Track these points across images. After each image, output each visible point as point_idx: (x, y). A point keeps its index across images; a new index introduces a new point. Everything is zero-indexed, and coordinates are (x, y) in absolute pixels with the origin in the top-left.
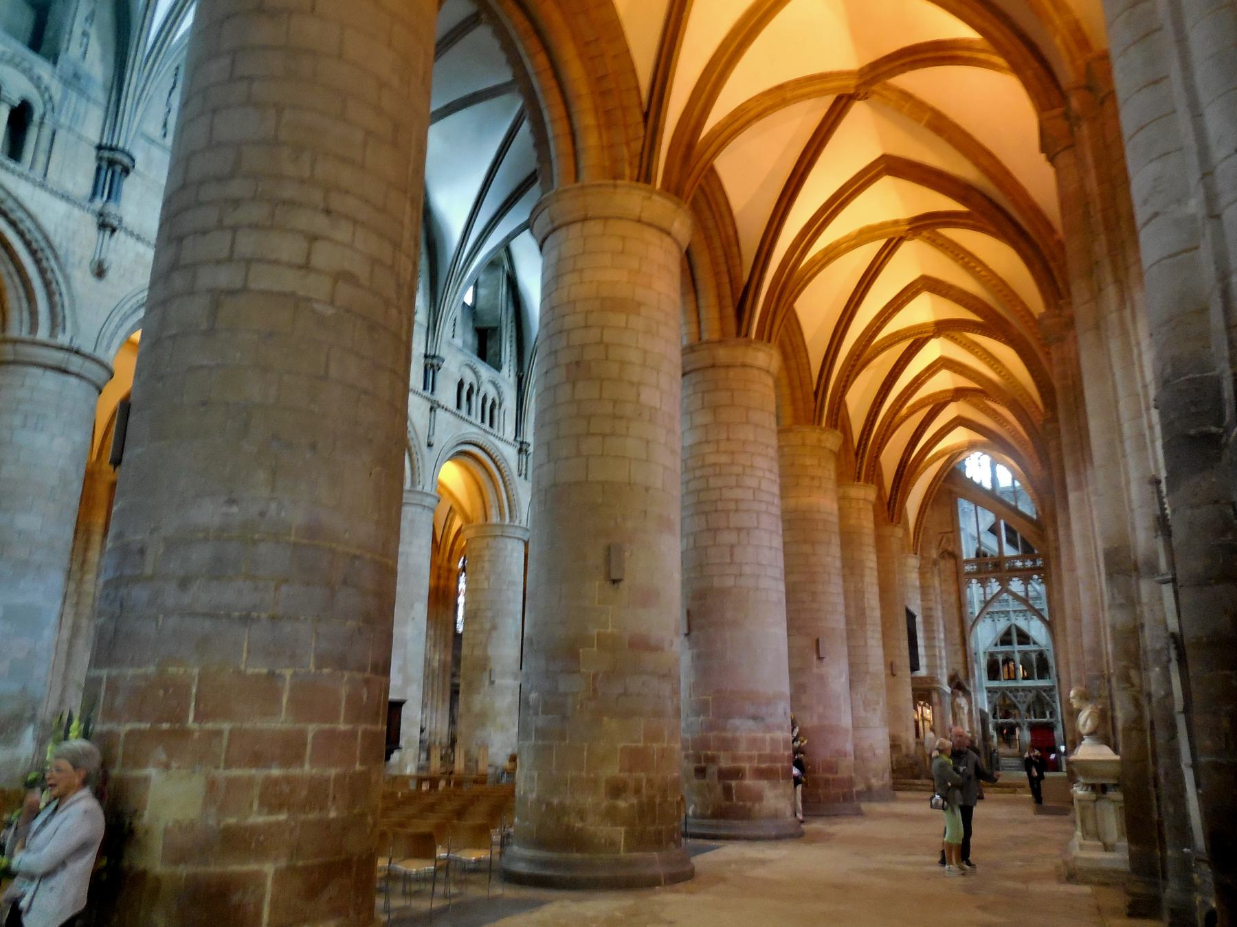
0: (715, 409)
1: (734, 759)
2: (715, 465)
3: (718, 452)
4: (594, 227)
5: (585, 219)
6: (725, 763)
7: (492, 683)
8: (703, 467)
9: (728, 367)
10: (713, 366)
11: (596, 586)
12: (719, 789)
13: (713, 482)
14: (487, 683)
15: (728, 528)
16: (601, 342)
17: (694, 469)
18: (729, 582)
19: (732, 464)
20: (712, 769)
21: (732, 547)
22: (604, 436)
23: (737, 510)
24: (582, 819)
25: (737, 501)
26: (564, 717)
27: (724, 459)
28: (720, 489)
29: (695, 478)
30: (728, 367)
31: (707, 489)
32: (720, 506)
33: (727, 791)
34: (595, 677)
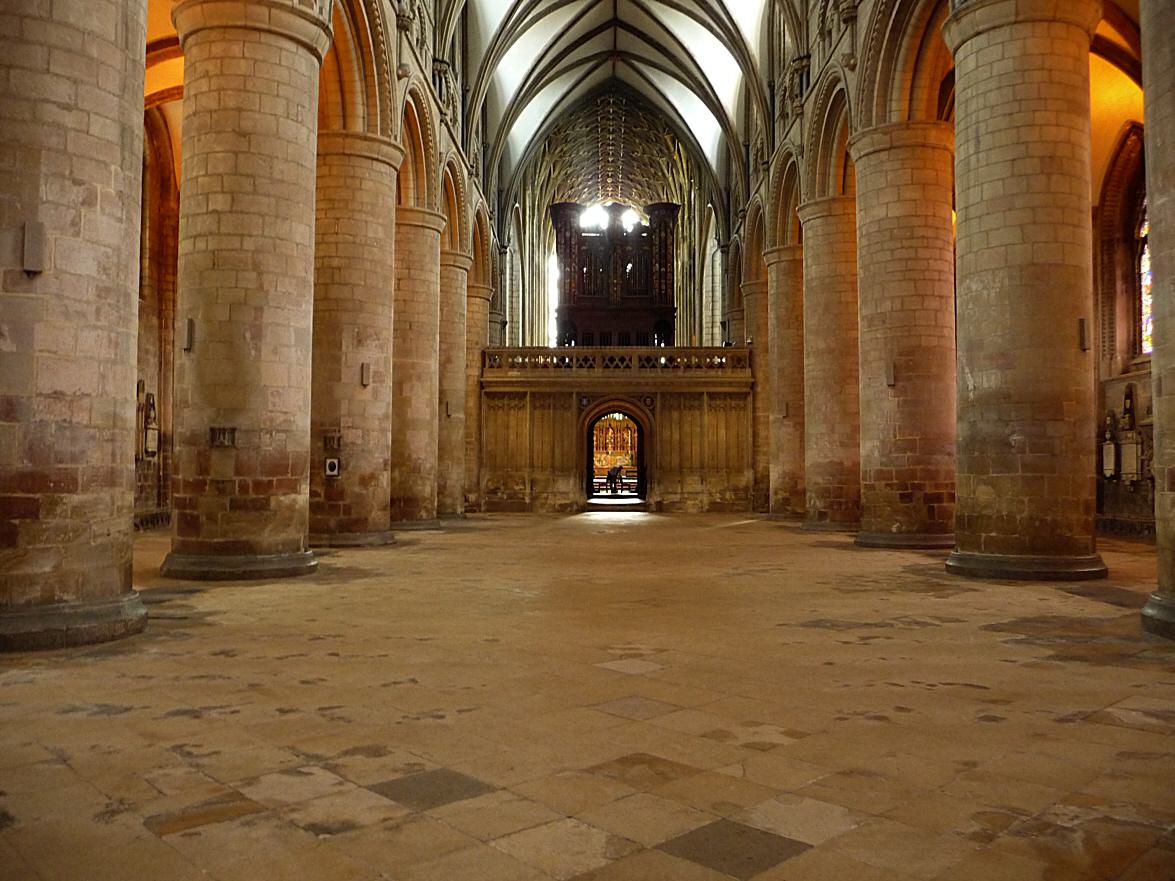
0: (924, 185)
1: (937, 486)
2: (923, 237)
3: (925, 226)
4: (1059, 29)
5: (1053, 20)
6: (929, 490)
7: (449, 416)
8: (912, 238)
9: (934, 148)
10: (923, 146)
11: (1074, 350)
12: (925, 508)
13: (922, 253)
14: (444, 415)
15: (933, 295)
16: (1069, 142)
17: (901, 239)
18: (934, 342)
19: (937, 238)
20: (919, 494)
21: (936, 311)
22: (1074, 226)
23: (940, 280)
24: (1071, 530)
25: (940, 272)
26: (1053, 455)
27: (930, 233)
28: (928, 259)
29: (902, 248)
30: (934, 148)
31: (916, 259)
32: (927, 275)
33: (931, 510)
34: (1075, 424)
